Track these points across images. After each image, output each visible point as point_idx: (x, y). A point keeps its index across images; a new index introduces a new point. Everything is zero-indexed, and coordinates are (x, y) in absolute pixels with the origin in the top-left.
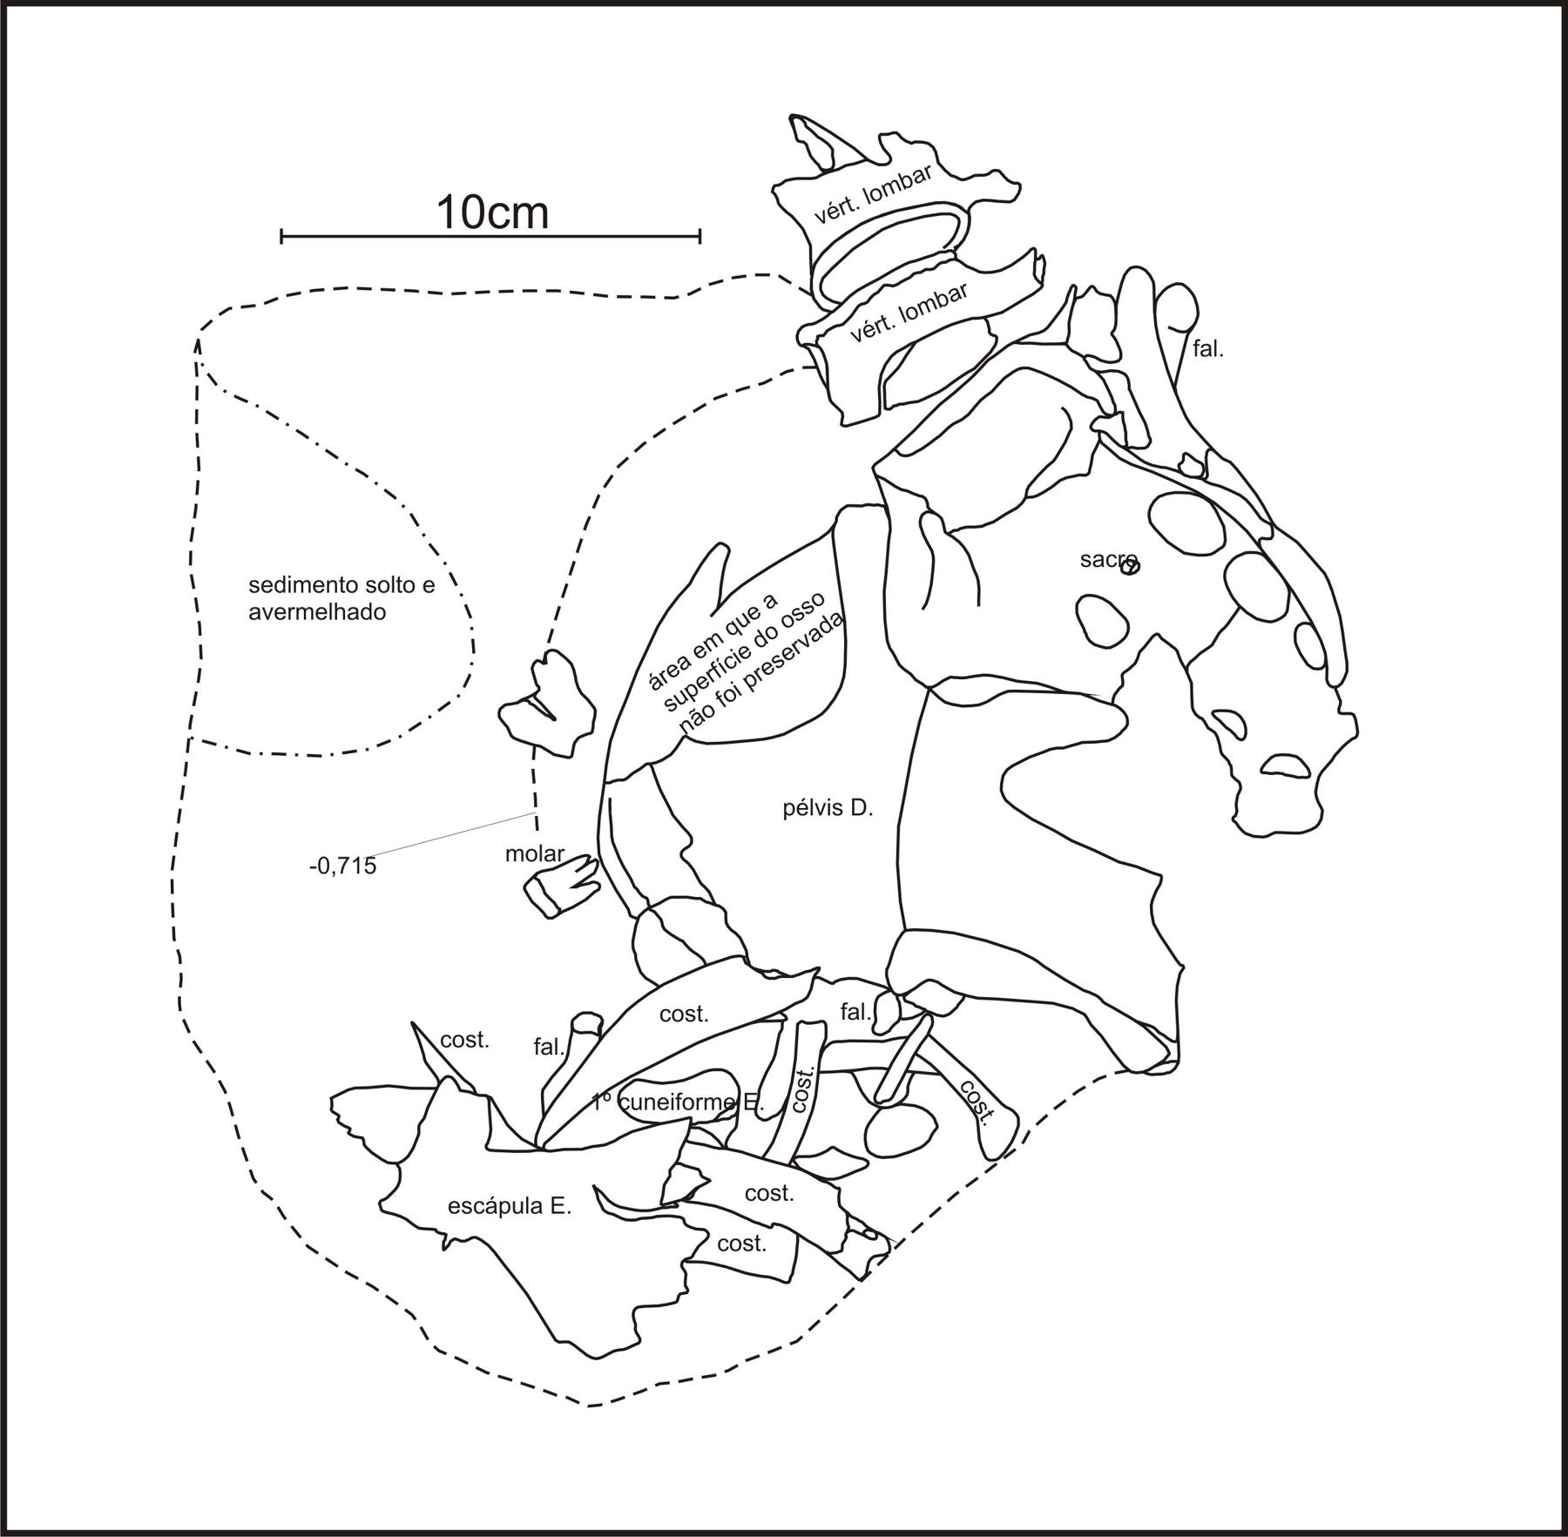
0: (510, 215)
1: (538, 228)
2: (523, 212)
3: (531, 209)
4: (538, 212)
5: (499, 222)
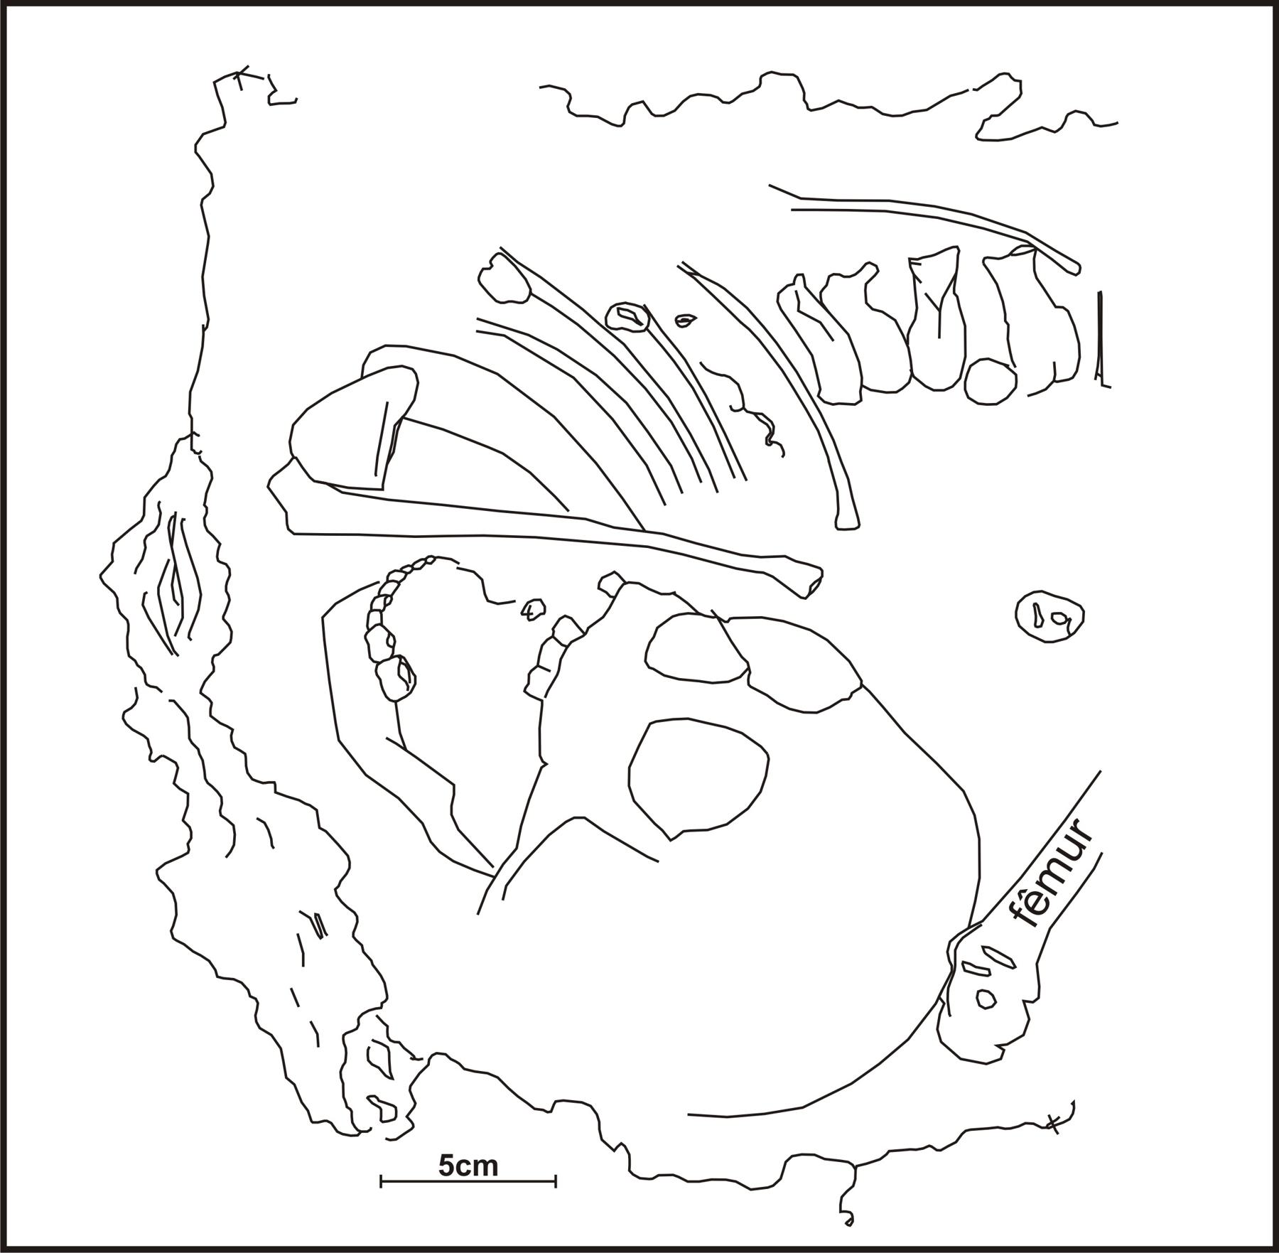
0: (471, 1167)
1: (490, 1176)
2: (481, 1166)
4: (491, 1166)
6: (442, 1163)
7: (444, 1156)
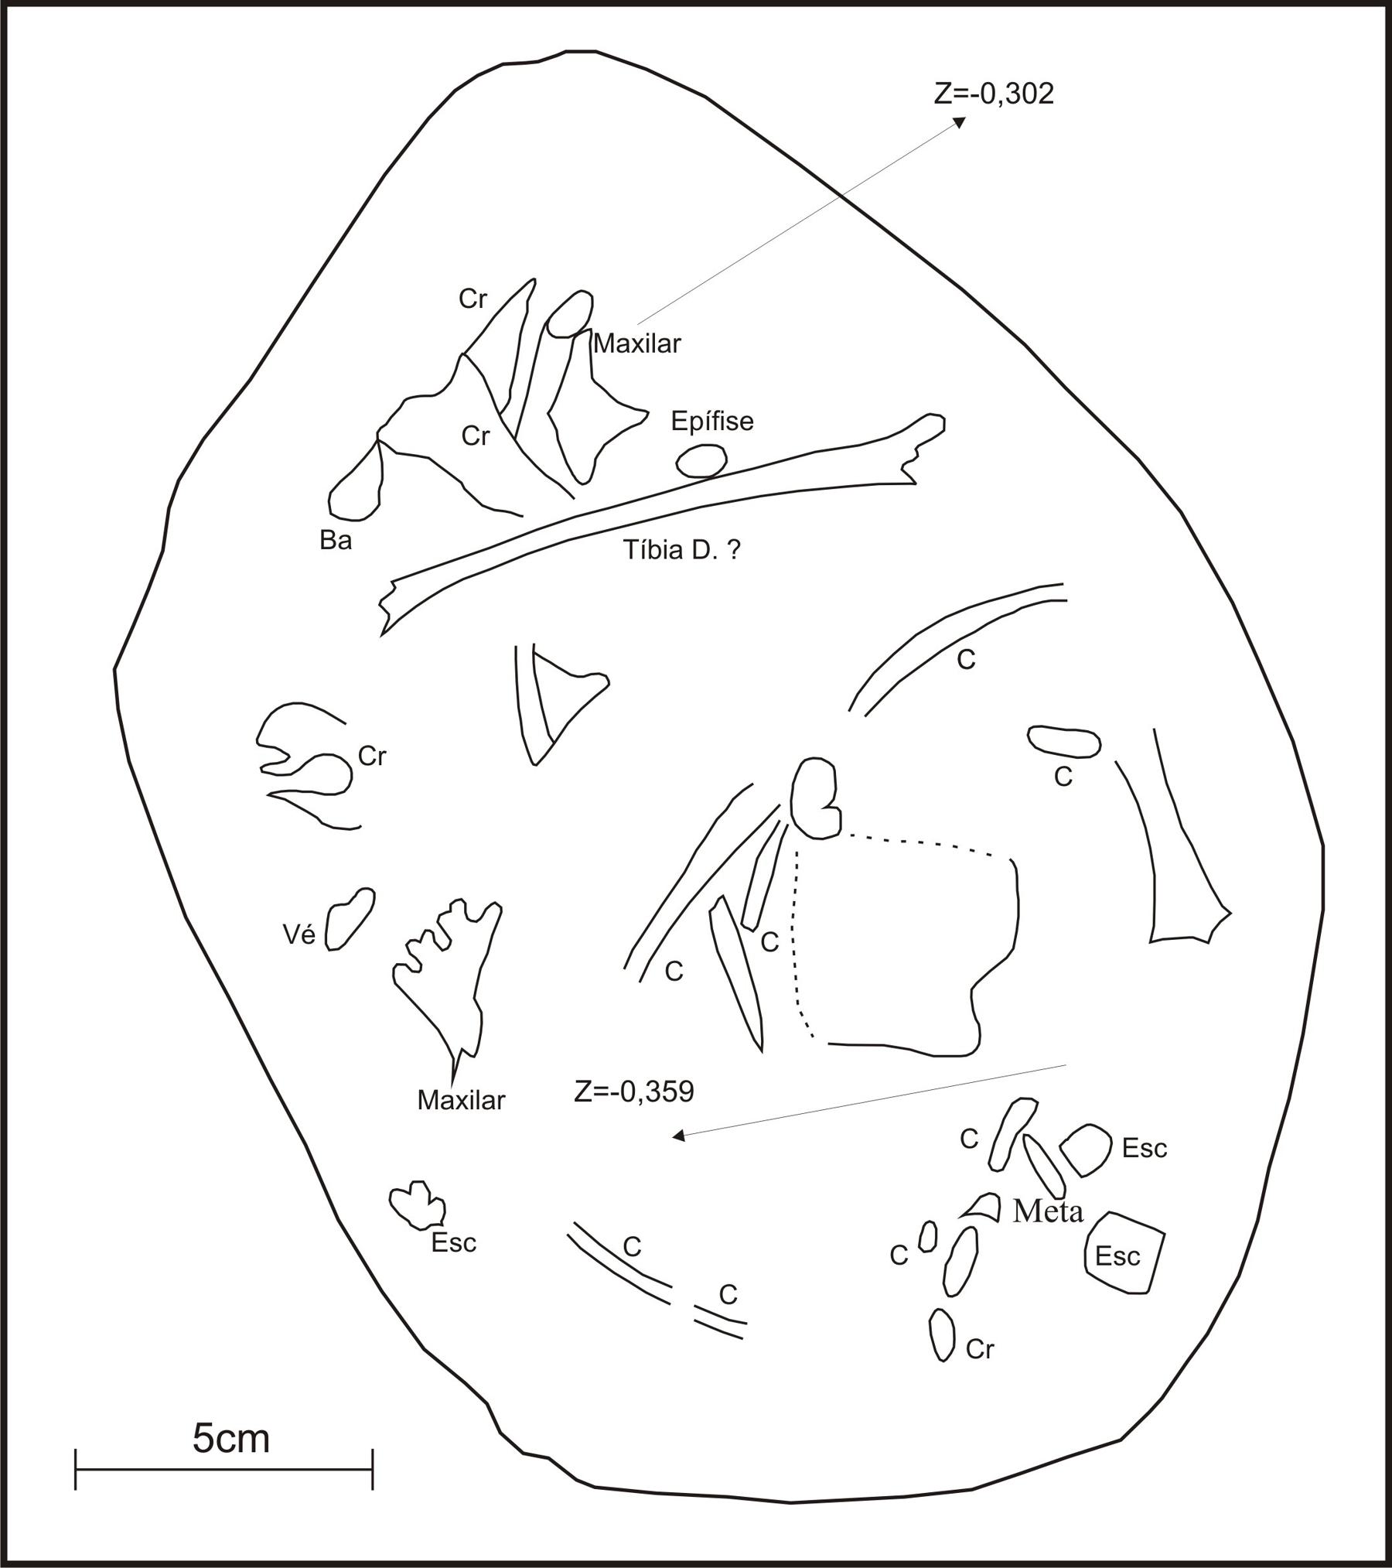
0: (236, 1441)
2: (247, 1438)
3: (254, 1435)
4: (260, 1438)
5: (226, 1445)
6: (197, 1435)
7: (199, 1425)
